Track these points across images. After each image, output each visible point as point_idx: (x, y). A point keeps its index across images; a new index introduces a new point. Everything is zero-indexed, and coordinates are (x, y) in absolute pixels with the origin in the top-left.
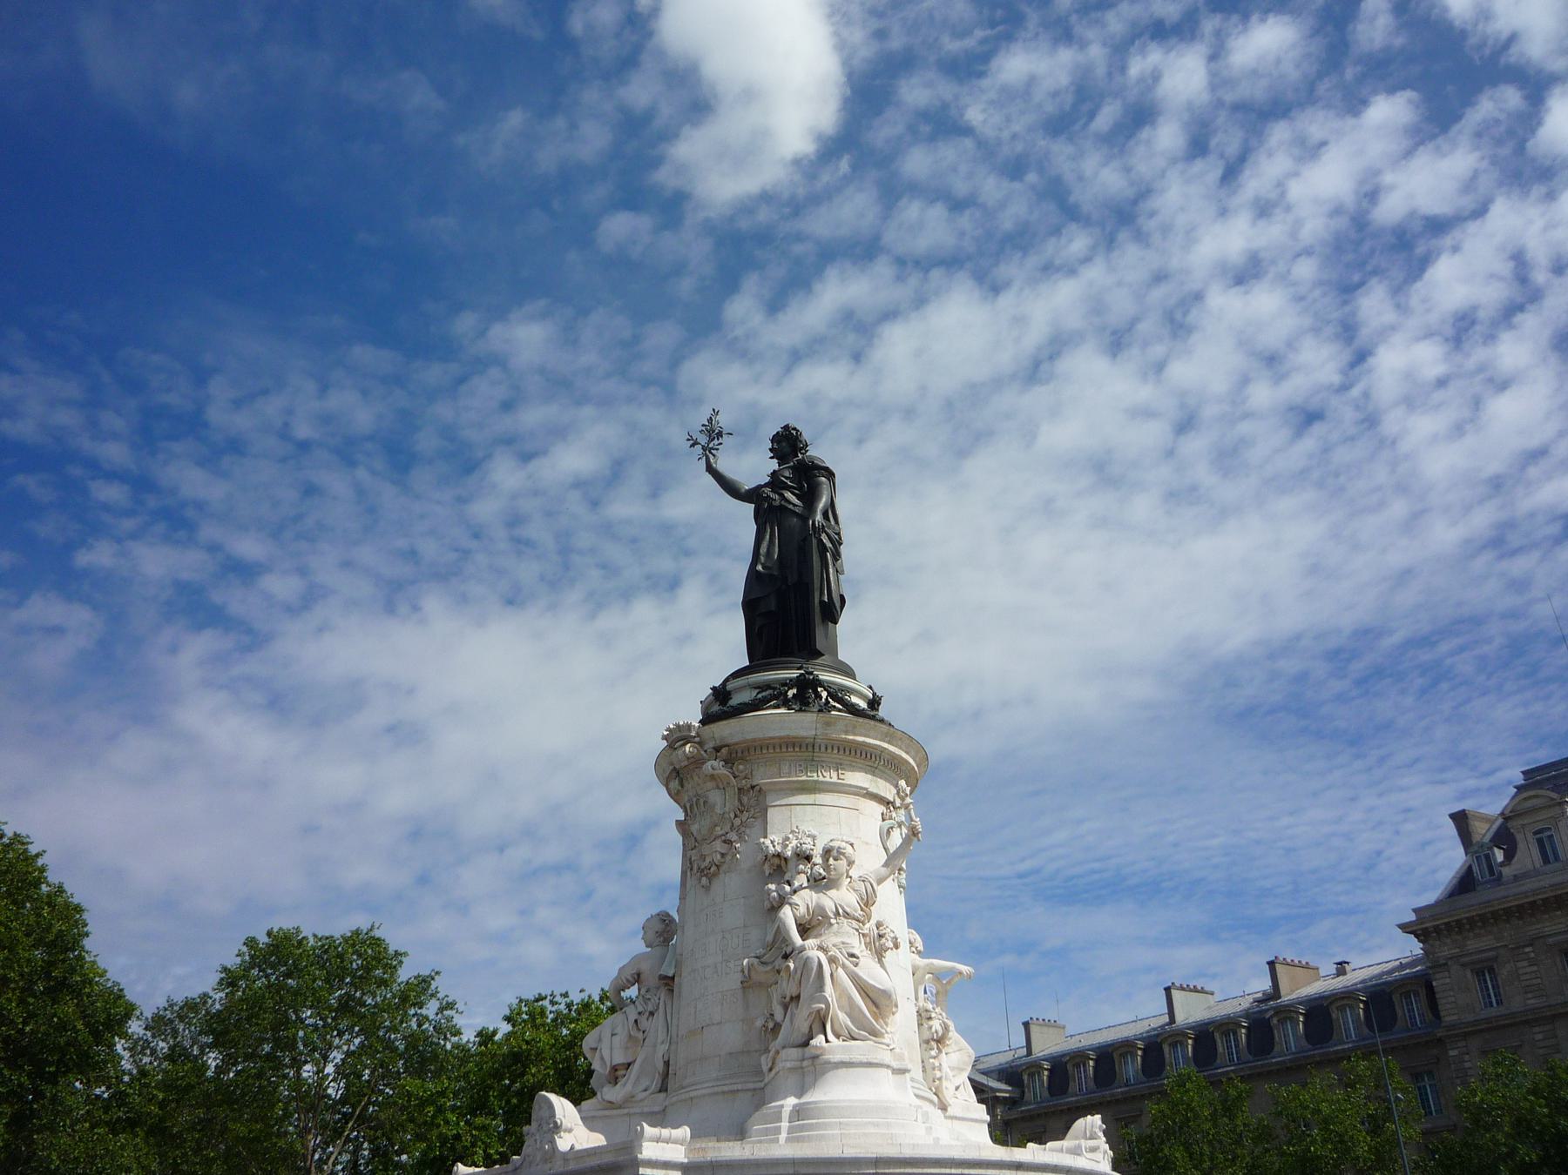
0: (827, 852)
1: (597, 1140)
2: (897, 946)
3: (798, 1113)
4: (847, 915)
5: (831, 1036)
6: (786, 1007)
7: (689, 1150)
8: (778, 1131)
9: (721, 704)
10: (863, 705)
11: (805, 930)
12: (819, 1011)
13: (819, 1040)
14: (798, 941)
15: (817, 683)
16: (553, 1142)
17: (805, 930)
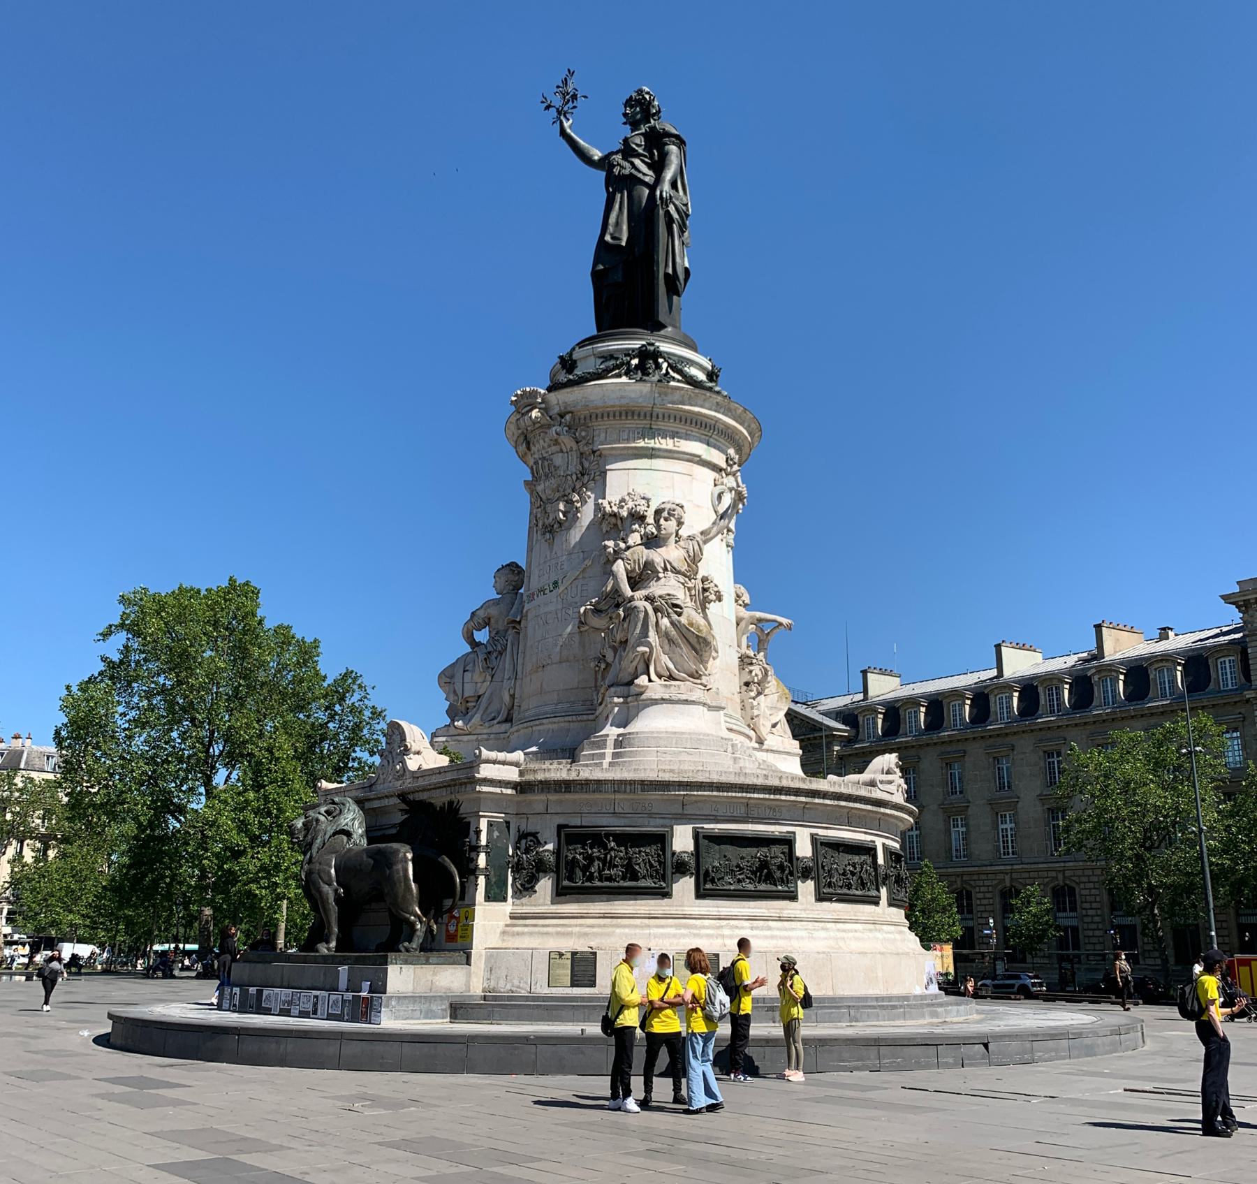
0: (658, 512)
1: (444, 761)
2: (719, 599)
3: (619, 743)
4: (677, 572)
5: (653, 677)
6: (615, 650)
7: (521, 773)
8: (603, 756)
9: (568, 371)
10: (701, 376)
11: (635, 583)
12: (643, 653)
13: (642, 680)
14: (628, 592)
15: (657, 354)
16: (403, 762)
17: (635, 583)
